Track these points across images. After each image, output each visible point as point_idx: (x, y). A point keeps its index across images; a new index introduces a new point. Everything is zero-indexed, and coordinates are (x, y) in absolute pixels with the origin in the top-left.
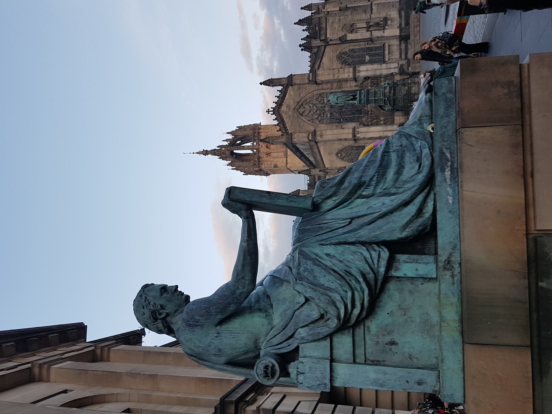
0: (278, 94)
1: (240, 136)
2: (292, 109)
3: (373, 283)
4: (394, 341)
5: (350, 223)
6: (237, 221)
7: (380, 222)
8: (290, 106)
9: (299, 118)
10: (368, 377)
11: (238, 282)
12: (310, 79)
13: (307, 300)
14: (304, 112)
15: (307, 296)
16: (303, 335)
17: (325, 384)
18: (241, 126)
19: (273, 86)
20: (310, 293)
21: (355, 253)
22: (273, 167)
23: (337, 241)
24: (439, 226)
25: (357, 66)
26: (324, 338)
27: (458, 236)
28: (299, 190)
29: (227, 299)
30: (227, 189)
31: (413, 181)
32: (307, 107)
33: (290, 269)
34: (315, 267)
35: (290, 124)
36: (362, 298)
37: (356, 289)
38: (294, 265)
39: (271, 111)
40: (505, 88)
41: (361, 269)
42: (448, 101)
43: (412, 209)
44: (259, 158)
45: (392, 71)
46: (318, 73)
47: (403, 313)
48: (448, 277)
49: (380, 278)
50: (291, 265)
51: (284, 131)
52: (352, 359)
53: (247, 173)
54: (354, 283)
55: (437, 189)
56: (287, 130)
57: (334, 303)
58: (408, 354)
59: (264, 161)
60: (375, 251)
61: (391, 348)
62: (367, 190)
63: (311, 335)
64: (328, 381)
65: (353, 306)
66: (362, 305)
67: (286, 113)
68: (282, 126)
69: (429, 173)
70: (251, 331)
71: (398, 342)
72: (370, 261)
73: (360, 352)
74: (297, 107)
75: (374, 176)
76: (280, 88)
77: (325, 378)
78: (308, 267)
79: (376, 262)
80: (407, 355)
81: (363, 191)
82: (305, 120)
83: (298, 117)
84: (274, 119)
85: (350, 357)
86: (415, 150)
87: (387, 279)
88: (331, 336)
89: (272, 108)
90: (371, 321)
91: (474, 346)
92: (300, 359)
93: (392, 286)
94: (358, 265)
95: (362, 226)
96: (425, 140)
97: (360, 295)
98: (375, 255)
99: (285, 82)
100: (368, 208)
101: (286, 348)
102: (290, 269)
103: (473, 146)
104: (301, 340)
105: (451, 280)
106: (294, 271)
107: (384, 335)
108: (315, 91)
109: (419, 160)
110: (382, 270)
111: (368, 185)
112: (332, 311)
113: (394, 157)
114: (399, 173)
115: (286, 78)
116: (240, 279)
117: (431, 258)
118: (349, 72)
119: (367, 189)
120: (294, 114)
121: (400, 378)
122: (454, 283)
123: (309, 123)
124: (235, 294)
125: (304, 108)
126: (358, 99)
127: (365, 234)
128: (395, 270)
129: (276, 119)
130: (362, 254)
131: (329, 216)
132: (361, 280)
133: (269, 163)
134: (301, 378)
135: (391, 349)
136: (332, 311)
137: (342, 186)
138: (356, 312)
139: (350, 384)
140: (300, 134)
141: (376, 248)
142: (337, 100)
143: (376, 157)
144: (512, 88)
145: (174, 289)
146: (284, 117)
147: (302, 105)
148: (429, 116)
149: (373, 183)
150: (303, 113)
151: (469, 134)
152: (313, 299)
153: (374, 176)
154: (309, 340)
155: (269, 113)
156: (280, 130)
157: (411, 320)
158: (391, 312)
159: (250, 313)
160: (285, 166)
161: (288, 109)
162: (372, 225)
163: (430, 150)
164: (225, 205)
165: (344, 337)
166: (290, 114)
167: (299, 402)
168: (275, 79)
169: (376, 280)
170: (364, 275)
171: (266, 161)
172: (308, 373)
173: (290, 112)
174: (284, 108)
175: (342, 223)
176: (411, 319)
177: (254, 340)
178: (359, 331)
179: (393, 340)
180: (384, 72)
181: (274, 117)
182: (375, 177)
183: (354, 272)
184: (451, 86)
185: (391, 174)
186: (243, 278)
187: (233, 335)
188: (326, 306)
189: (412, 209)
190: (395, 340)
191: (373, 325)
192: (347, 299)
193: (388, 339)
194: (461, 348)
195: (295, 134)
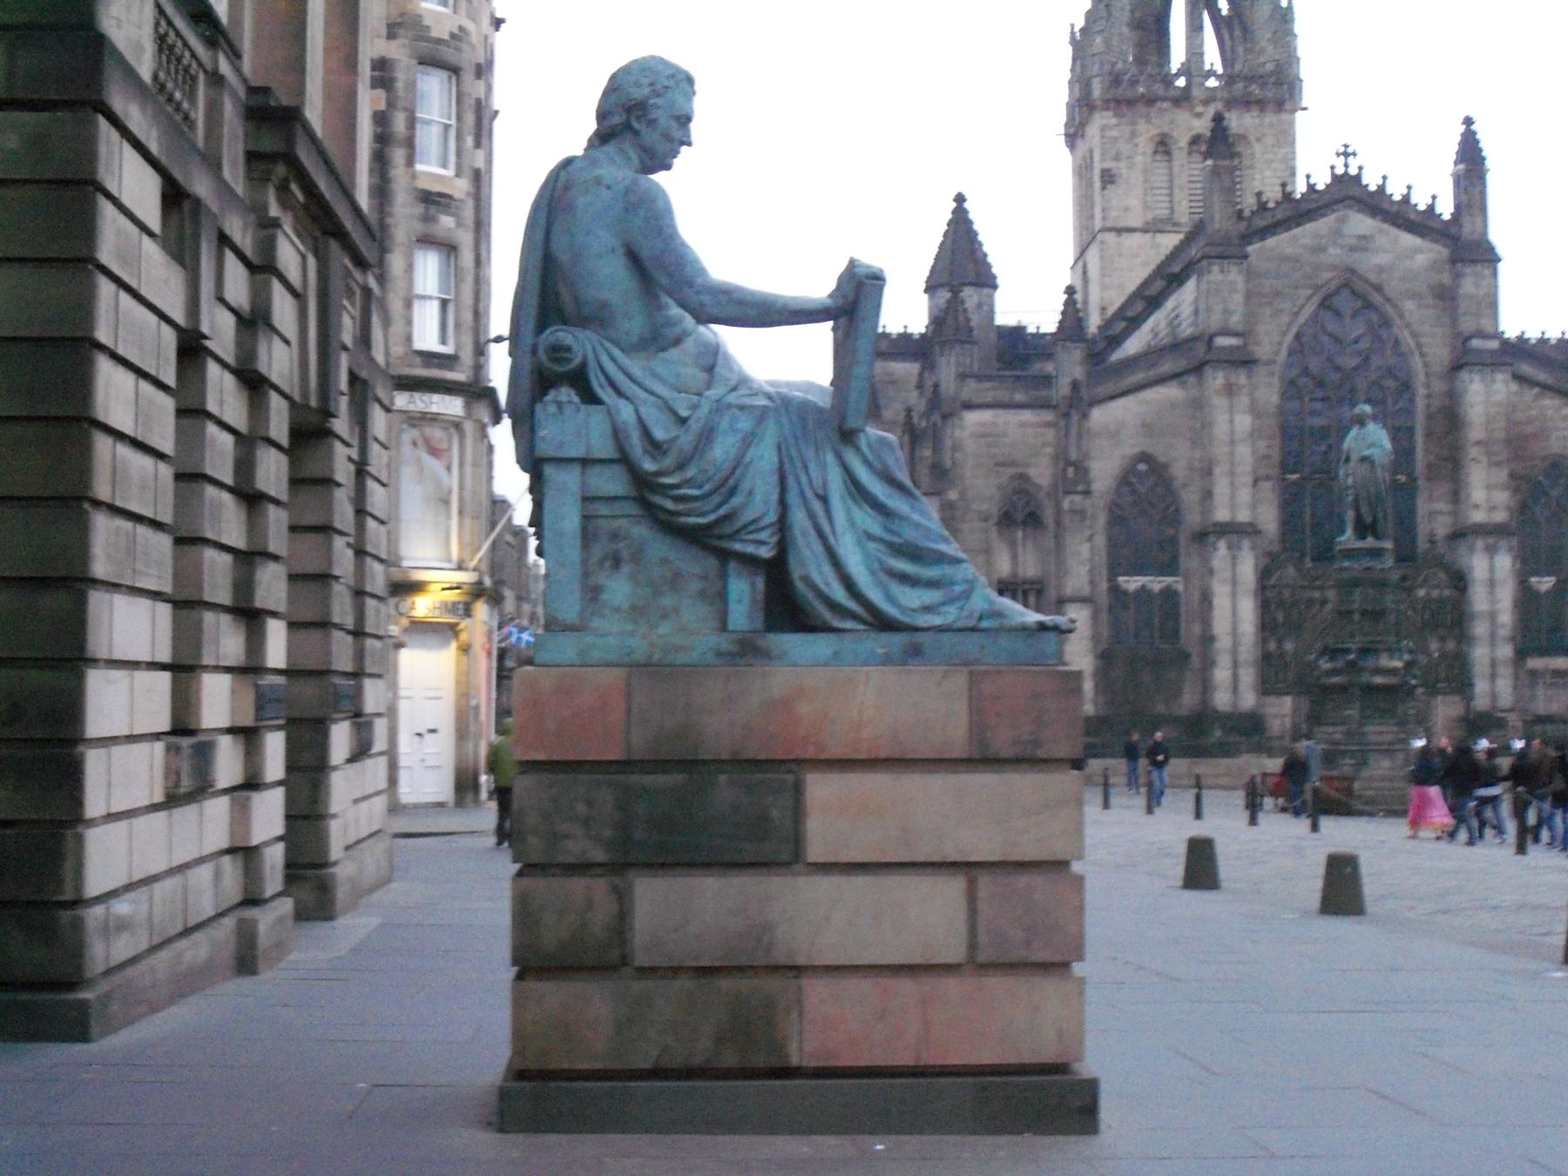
0: (1421, 201)
1: (1248, 13)
2: (1355, 260)
3: (716, 532)
5: (818, 496)
6: (820, 286)
7: (818, 548)
8: (1365, 249)
9: (1309, 292)
12: (1475, 343)
13: (683, 421)
14: (1338, 314)
15: (691, 422)
18: (1292, 20)
19: (1457, 179)
20: (695, 426)
22: (1107, 165)
24: (811, 637)
25: (1515, 541)
26: (621, 448)
28: (995, 287)
30: (881, 271)
32: (1356, 329)
33: (734, 389)
35: (1289, 250)
38: (743, 396)
39: (1346, 166)
43: (839, 594)
44: (1150, 101)
45: (1481, 686)
46: (1500, 377)
49: (725, 544)
50: (742, 391)
51: (1259, 223)
52: (589, 495)
53: (1081, 45)
55: (873, 635)
56: (1263, 239)
57: (681, 467)
59: (1133, 123)
60: (771, 537)
66: (679, 514)
67: (1337, 233)
68: (1280, 215)
69: (900, 622)
72: (751, 528)
73: (603, 509)
74: (1359, 286)
76: (1446, 209)
82: (1302, 319)
83: (1317, 288)
84: (1312, 181)
85: (593, 492)
86: (943, 604)
87: (725, 556)
88: (624, 459)
89: (1360, 168)
90: (651, 528)
92: (583, 407)
93: (712, 563)
95: (812, 516)
96: (959, 619)
98: (764, 536)
99: (1467, 230)
101: (597, 382)
102: (734, 389)
106: (732, 398)
108: (1426, 365)
110: (738, 547)
112: (669, 461)
113: (932, 572)
114: (903, 578)
115: (1485, 233)
117: (759, 624)
118: (1492, 508)
120: (1333, 267)
123: (1289, 338)
125: (1355, 315)
126: (1360, 544)
127: (798, 517)
129: (1311, 187)
130: (764, 514)
131: (830, 458)
132: (722, 512)
133: (1125, 148)
134: (553, 409)
136: (669, 461)
138: (669, 505)
140: (1238, 299)
141: (775, 539)
142: (1364, 459)
143: (935, 541)
145: (685, 139)
146: (1322, 225)
147: (1368, 305)
149: (887, 537)
150: (1329, 308)
151: (958, 682)
152: (687, 431)
153: (899, 535)
155: (1338, 155)
156: (1262, 207)
160: (1109, 224)
161: (1354, 241)
162: (813, 532)
164: (852, 264)
166: (1331, 251)
167: (287, 342)
168: (1484, 185)
169: (720, 537)
170: (728, 517)
171: (1134, 134)
173: (1339, 252)
174: (1360, 223)
175: (817, 482)
178: (632, 509)
180: (1480, 654)
181: (1322, 181)
183: (736, 501)
189: (839, 594)
191: (641, 531)
193: (625, 554)
195: (1240, 272)
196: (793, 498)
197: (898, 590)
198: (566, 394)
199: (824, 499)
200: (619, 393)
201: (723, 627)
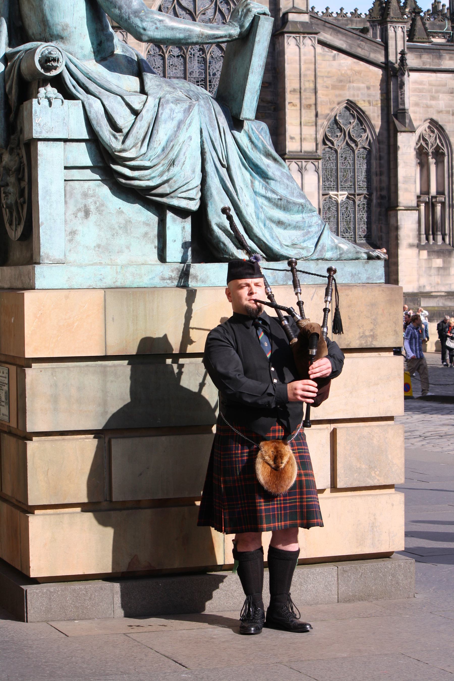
4: (90, 214)
5: (223, 165)
10: (51, 183)
11: (151, 22)
13: (136, 113)
15: (144, 112)
16: (94, 106)
17: (41, 133)
21: (194, 172)
23: (207, 150)
27: (214, 285)
29: (126, 5)
31: (273, 238)
34: (175, 123)
36: (143, 179)
37: (153, 172)
40: (370, 332)
41: (174, 178)
42: (358, 275)
47: (121, 226)
48: (171, 274)
49: (164, 200)
54: (160, 170)
58: (76, 230)
61: (81, 211)
62: (261, 186)
63: (97, 116)
64: (44, 136)
65: (133, 168)
70: (75, 32)
71: (89, 219)
73: (76, 174)
75: (277, 195)
77: (47, 132)
78: (175, 115)
79: (184, 195)
80: (75, 229)
81: (260, 182)
91: (103, 299)
92: (66, 101)
94: (179, 175)
97: (146, 176)
100: (241, 188)
103: (312, 299)
104: (89, 104)
105: (167, 276)
107: (96, 203)
109: (294, 245)
110: (175, 202)
111: (266, 188)
113: (297, 217)
114: (280, 223)
116: (156, 24)
119: (263, 186)
121: (54, 219)
122: (163, 279)
124: (135, 17)
128: (173, 218)
132: (165, 178)
134: (45, 102)
135: (79, 210)
137: (264, 155)
139: (42, 162)
144: (370, 339)
148: (340, 258)
149: (269, 194)
154: (90, 113)
157: (114, 234)
158: (122, 212)
159: (96, 30)
163: (306, 257)
165: (93, 155)
172: (52, 112)
176: (116, 234)
177: (63, 36)
179: (90, 212)
182: (274, 196)
184: (374, 279)
185: (278, 214)
186: (157, 28)
187: (72, 7)
188: (134, 135)
190: (91, 215)
192: (142, 160)
193: (92, 208)
194: (94, 287)
196: (210, 168)
197: (278, 231)
198: (51, 91)
199: (228, 170)
200: (87, 91)
201: (162, 257)
